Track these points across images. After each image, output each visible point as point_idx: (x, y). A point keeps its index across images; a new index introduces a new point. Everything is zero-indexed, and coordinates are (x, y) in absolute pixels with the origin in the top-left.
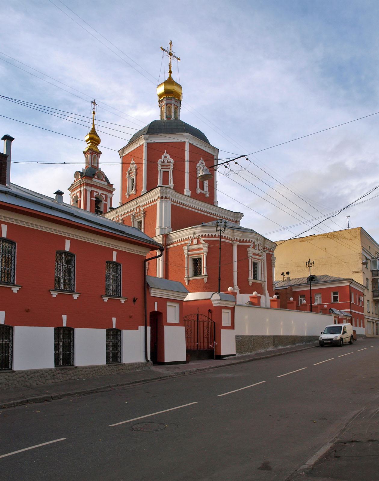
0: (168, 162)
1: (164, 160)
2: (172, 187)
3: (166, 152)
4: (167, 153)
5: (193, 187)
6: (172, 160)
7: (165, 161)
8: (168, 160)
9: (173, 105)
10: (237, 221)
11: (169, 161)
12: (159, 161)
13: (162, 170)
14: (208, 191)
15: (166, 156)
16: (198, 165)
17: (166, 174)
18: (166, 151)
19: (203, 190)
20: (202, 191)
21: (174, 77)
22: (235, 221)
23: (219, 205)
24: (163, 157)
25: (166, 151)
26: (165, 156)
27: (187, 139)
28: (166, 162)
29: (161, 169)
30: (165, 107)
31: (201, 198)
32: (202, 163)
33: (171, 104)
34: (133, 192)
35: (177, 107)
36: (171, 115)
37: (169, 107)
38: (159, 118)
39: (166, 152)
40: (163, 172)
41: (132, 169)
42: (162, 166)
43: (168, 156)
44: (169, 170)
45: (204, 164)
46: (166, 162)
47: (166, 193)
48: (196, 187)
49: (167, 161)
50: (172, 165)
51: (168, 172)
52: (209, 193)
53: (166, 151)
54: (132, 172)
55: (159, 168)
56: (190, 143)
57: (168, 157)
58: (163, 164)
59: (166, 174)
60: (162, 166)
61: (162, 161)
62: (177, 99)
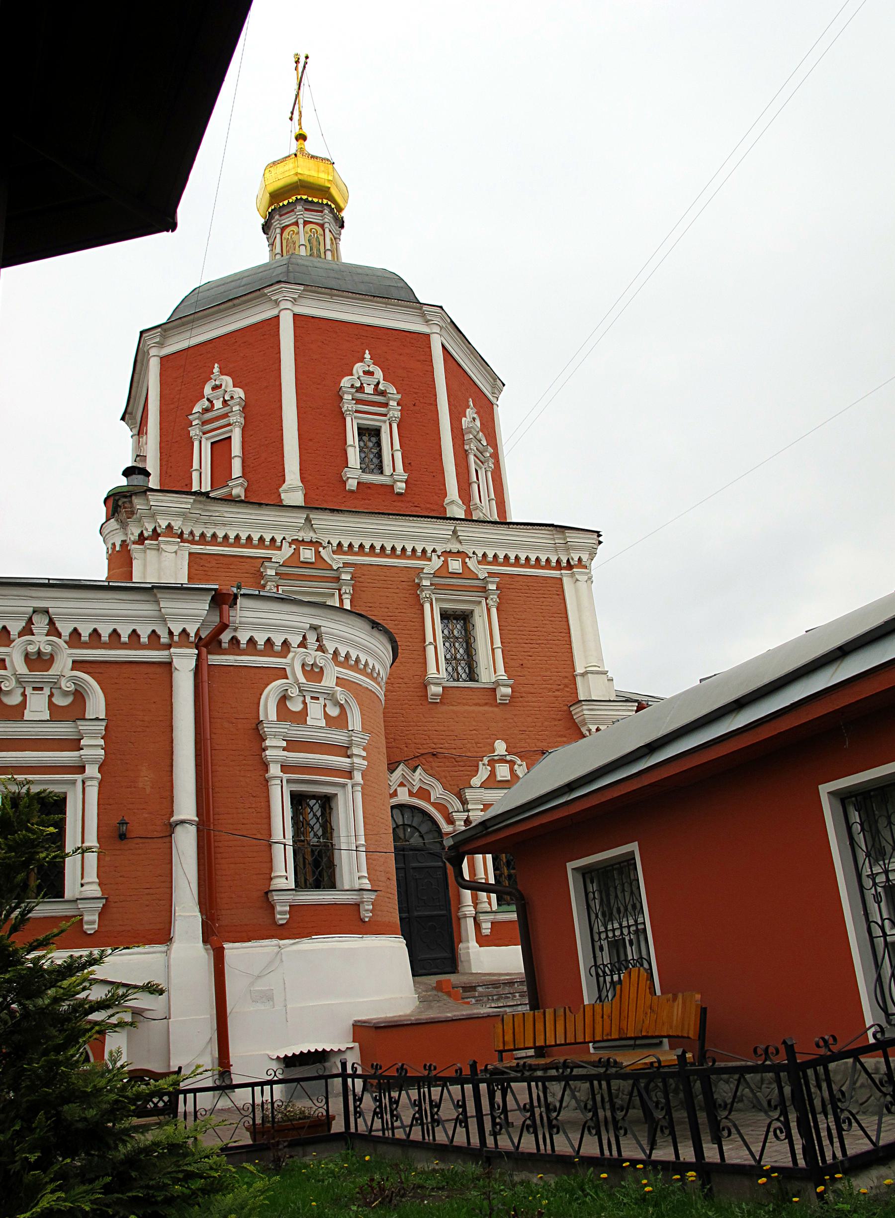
6: (240, 393)
11: (227, 398)
12: (197, 408)
13: (207, 439)
15: (217, 383)
16: (345, 382)
17: (221, 447)
19: (380, 469)
28: (218, 404)
40: (212, 443)
43: (227, 381)
44: (231, 431)
46: (218, 404)
47: (153, 516)
49: (222, 399)
55: (194, 432)
57: (223, 387)
58: (208, 416)
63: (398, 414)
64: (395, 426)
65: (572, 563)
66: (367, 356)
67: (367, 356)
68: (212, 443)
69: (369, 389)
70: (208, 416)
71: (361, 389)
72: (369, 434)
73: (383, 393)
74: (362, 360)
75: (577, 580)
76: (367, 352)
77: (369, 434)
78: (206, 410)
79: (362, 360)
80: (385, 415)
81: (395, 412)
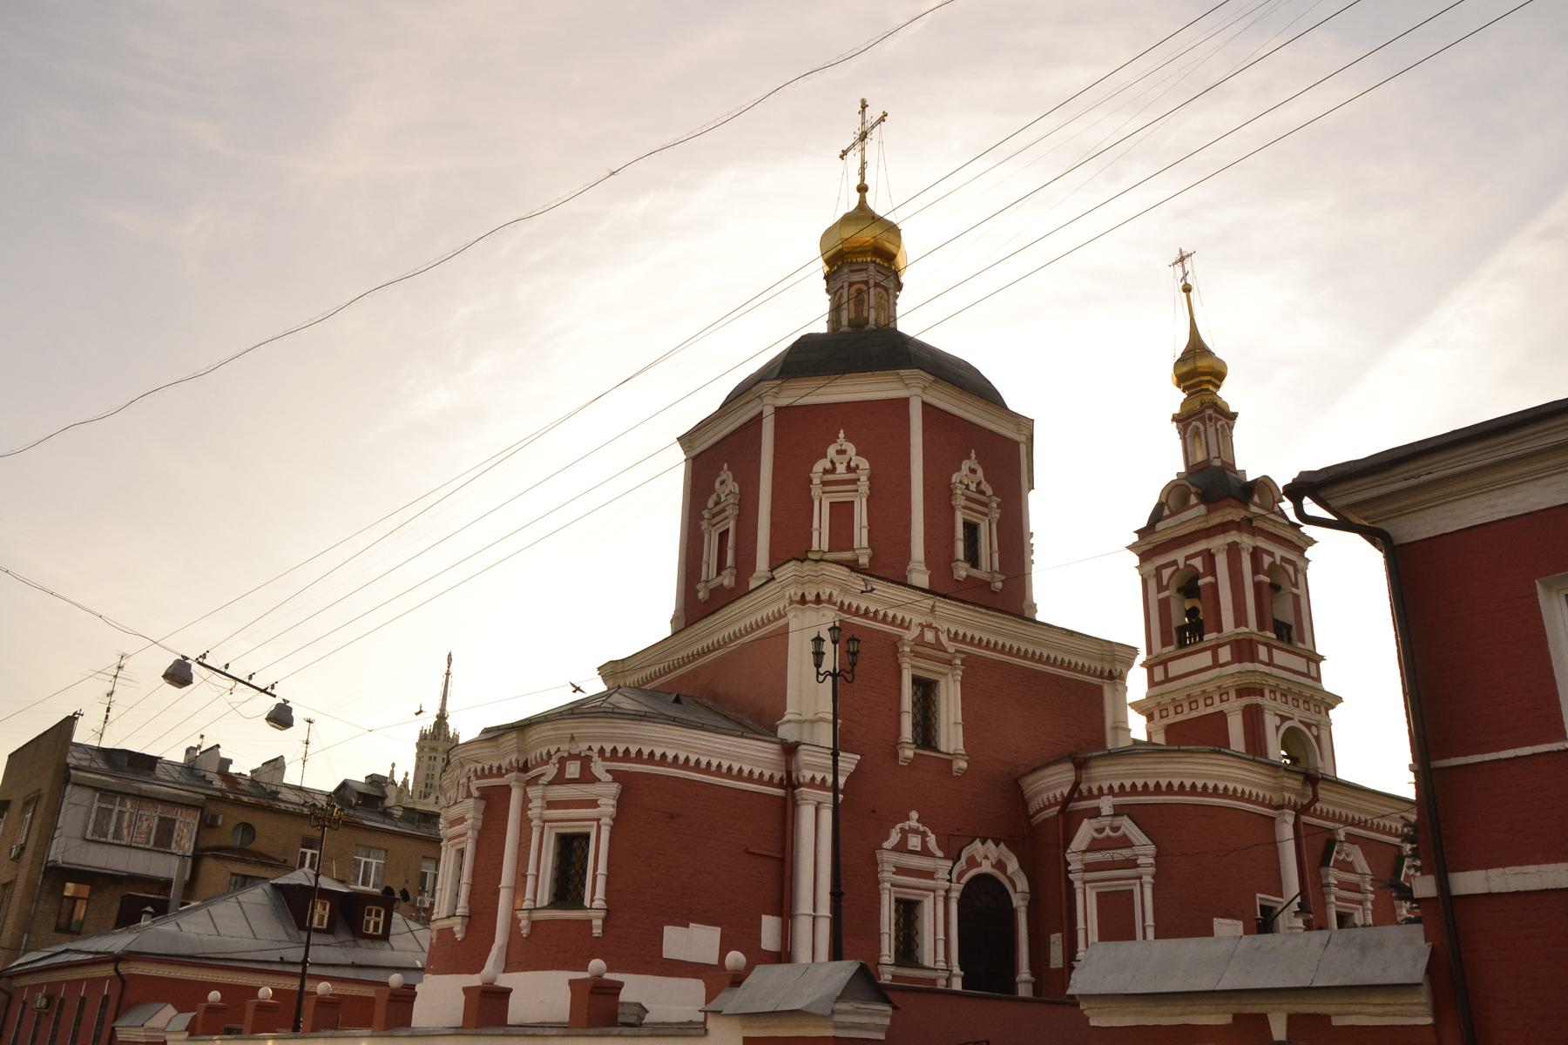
0: (849, 469)
1: (832, 462)
2: (864, 560)
3: (842, 435)
4: (848, 438)
5: (939, 558)
6: (864, 464)
7: (837, 465)
8: (849, 463)
9: (872, 282)
10: (1115, 674)
12: (819, 467)
13: (827, 498)
14: (996, 566)
15: (843, 448)
16: (955, 478)
17: (843, 513)
18: (844, 433)
20: (974, 573)
21: (879, 204)
22: (1106, 674)
23: (1039, 617)
24: (832, 451)
25: (842, 431)
26: (839, 448)
27: (913, 390)
28: (841, 468)
29: (823, 493)
30: (845, 292)
31: (976, 595)
32: (973, 471)
33: (866, 283)
34: (728, 580)
35: (886, 289)
36: (865, 315)
37: (860, 292)
38: (822, 327)
39: (842, 435)
40: (831, 503)
41: (723, 499)
42: (824, 483)
43: (851, 449)
45: (980, 472)
46: (841, 468)
48: (952, 558)
49: (845, 464)
50: (864, 478)
51: (853, 502)
52: (1003, 577)
53: (842, 431)
54: (723, 510)
55: (816, 491)
56: (924, 403)
58: (829, 477)
59: (843, 513)
60: (824, 483)
61: (829, 466)
62: (883, 266)
63: (997, 516)
64: (994, 526)
65: (1115, 674)
66: (973, 455)
67: (973, 455)
68: (831, 503)
69: (973, 487)
70: (829, 477)
71: (967, 487)
72: (971, 529)
73: (983, 493)
74: (969, 457)
75: (1117, 690)
76: (973, 451)
77: (971, 529)
78: (826, 472)
79: (969, 457)
80: (986, 515)
81: (996, 515)
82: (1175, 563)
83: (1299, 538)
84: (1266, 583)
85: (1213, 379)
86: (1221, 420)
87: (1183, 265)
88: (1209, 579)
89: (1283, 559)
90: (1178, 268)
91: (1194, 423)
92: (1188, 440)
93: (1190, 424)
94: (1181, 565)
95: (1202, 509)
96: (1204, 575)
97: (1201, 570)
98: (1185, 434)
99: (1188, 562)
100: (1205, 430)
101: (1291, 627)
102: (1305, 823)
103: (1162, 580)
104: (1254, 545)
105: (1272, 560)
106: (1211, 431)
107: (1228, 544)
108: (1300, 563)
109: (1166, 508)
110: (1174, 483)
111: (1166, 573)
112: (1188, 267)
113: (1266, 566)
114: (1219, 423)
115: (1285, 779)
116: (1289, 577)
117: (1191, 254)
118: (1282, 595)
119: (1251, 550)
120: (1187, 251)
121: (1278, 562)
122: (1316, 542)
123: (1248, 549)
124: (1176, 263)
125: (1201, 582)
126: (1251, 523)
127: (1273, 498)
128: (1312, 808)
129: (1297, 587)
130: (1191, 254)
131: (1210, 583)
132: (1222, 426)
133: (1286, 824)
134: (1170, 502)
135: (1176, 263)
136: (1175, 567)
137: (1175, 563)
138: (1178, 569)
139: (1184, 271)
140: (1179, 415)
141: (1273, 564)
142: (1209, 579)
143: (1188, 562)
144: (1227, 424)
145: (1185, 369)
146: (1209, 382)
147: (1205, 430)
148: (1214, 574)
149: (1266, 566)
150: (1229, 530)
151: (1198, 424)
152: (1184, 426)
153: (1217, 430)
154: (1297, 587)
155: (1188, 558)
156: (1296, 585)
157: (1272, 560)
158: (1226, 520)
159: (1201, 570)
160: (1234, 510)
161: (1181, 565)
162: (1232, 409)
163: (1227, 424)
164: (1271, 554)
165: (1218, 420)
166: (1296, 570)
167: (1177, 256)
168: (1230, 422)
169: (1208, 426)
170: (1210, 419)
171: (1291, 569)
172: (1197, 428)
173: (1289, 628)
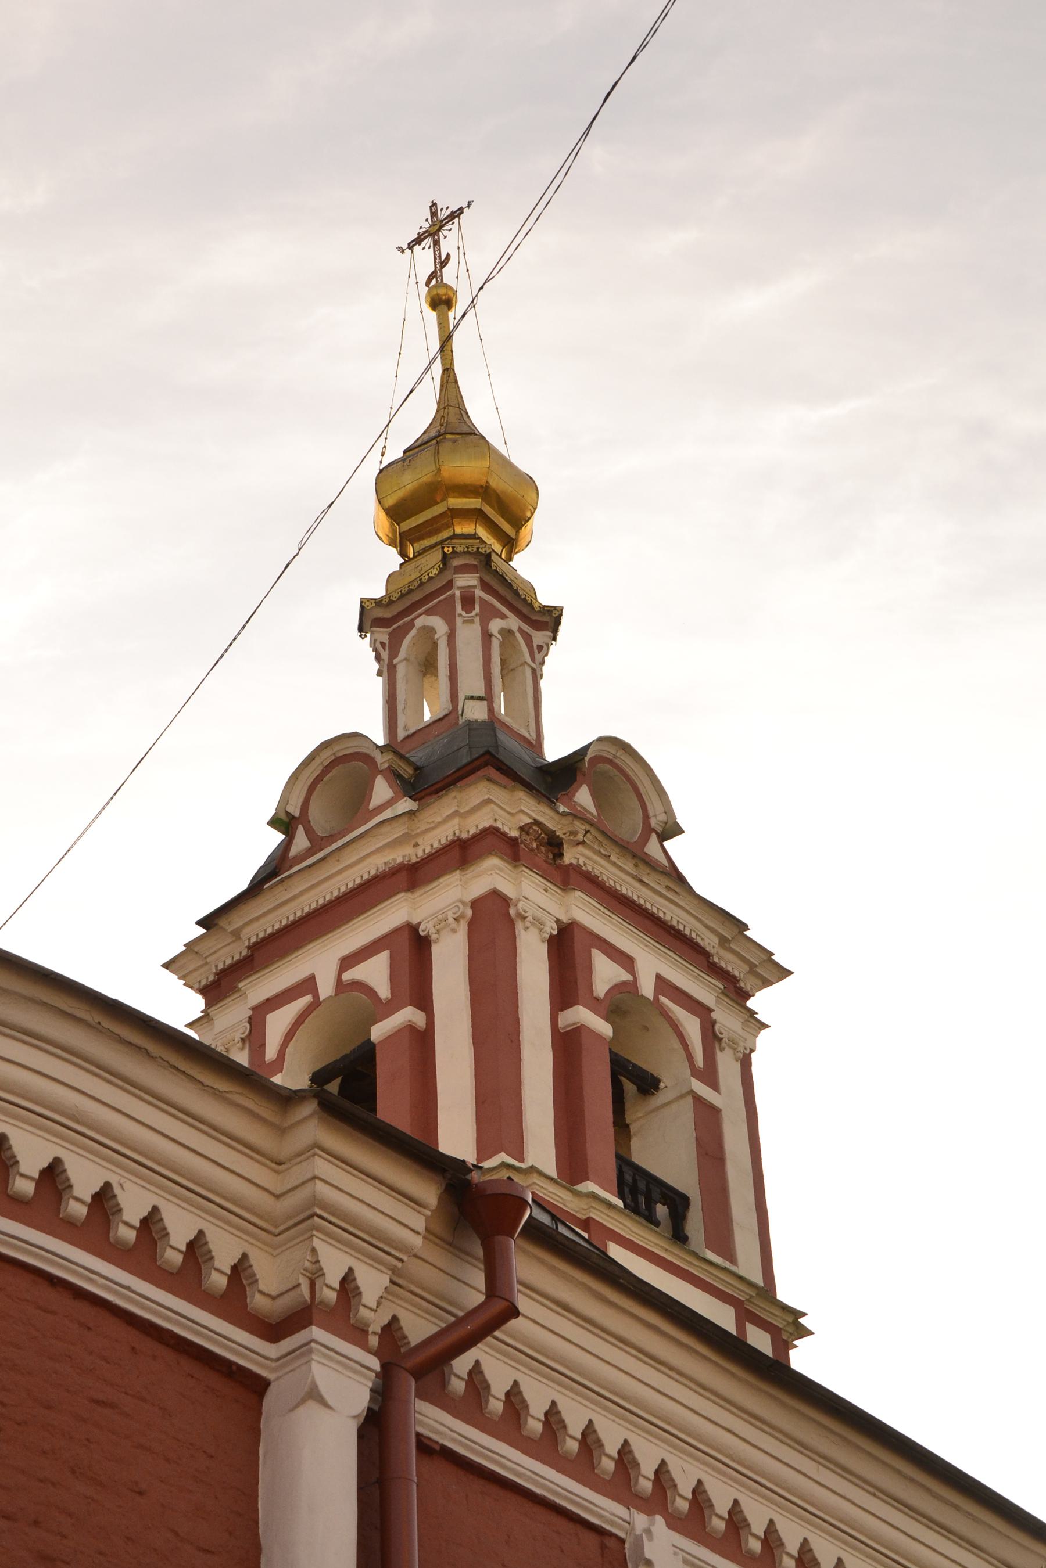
82: (309, 984)
83: (723, 941)
84: (598, 1036)
85: (488, 510)
86: (504, 617)
87: (437, 243)
88: (408, 1015)
89: (662, 984)
90: (424, 257)
91: (419, 622)
92: (401, 670)
93: (411, 625)
94: (326, 989)
95: (405, 805)
96: (389, 1008)
97: (384, 991)
98: (394, 652)
99: (347, 976)
100: (451, 636)
101: (685, 1200)
102: (426, 1448)
103: (263, 1045)
104: (565, 919)
105: (631, 978)
106: (469, 635)
107: (475, 904)
108: (726, 1019)
109: (300, 828)
110: (327, 757)
111: (278, 1023)
112: (448, 245)
113: (601, 988)
114: (496, 626)
115: (322, 1166)
116: (690, 1058)
117: (461, 210)
118: (658, 1108)
119: (551, 928)
120: (447, 204)
121: (647, 988)
122: (784, 973)
123: (538, 923)
124: (418, 240)
125: (378, 1032)
126: (561, 855)
127: (646, 817)
128: (462, 1364)
129: (714, 1086)
130: (461, 210)
131: (410, 1028)
132: (507, 633)
133: (312, 1406)
134: (315, 813)
135: (418, 240)
136: (307, 999)
137: (309, 984)
138: (316, 1003)
139: (437, 255)
140: (378, 602)
141: (629, 988)
142: (408, 1015)
143: (347, 976)
144: (528, 639)
145: (409, 482)
146: (478, 515)
147: (451, 636)
148: (423, 1000)
149: (601, 988)
150: (480, 857)
151: (438, 624)
152: (390, 634)
153: (487, 637)
154: (714, 1086)
155: (348, 962)
156: (709, 1076)
157: (625, 976)
158: (472, 831)
159: (384, 991)
160: (498, 794)
161: (326, 989)
162: (545, 598)
163: (528, 639)
164: (626, 961)
165: (489, 614)
166: (711, 1036)
167: (421, 221)
168: (539, 637)
169: (459, 621)
170: (468, 601)
171: (692, 1026)
172: (430, 631)
173: (678, 1203)
